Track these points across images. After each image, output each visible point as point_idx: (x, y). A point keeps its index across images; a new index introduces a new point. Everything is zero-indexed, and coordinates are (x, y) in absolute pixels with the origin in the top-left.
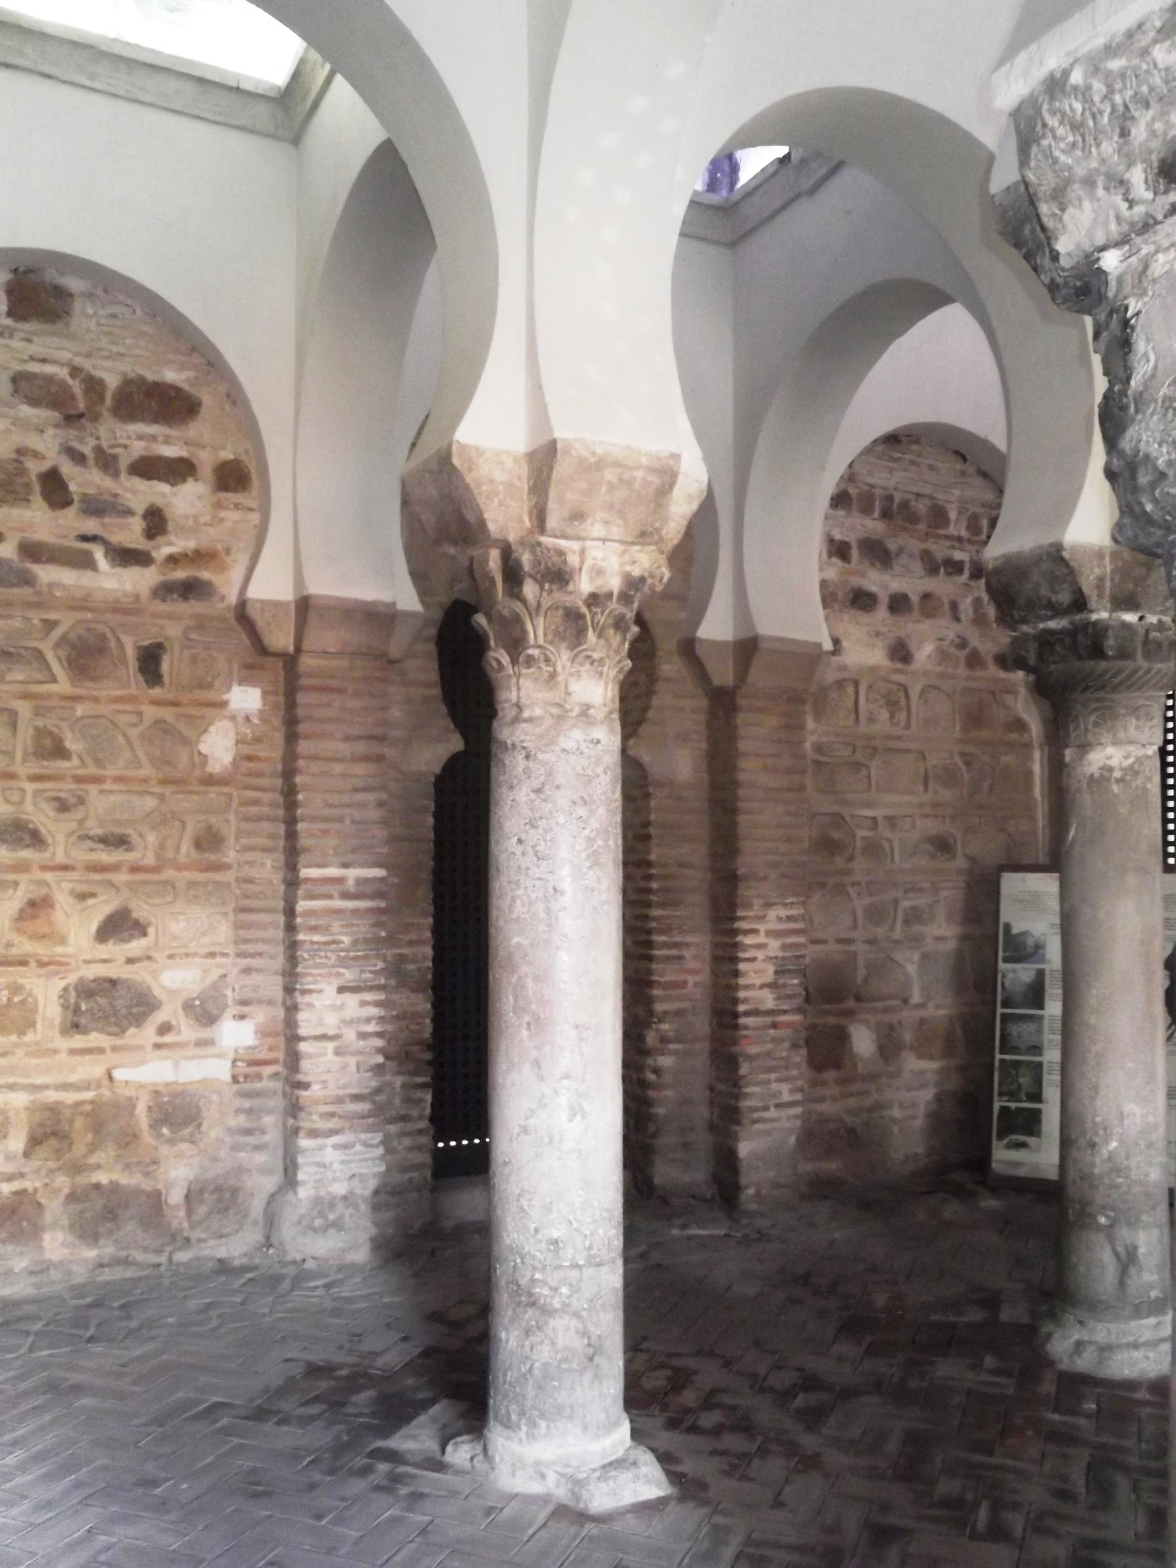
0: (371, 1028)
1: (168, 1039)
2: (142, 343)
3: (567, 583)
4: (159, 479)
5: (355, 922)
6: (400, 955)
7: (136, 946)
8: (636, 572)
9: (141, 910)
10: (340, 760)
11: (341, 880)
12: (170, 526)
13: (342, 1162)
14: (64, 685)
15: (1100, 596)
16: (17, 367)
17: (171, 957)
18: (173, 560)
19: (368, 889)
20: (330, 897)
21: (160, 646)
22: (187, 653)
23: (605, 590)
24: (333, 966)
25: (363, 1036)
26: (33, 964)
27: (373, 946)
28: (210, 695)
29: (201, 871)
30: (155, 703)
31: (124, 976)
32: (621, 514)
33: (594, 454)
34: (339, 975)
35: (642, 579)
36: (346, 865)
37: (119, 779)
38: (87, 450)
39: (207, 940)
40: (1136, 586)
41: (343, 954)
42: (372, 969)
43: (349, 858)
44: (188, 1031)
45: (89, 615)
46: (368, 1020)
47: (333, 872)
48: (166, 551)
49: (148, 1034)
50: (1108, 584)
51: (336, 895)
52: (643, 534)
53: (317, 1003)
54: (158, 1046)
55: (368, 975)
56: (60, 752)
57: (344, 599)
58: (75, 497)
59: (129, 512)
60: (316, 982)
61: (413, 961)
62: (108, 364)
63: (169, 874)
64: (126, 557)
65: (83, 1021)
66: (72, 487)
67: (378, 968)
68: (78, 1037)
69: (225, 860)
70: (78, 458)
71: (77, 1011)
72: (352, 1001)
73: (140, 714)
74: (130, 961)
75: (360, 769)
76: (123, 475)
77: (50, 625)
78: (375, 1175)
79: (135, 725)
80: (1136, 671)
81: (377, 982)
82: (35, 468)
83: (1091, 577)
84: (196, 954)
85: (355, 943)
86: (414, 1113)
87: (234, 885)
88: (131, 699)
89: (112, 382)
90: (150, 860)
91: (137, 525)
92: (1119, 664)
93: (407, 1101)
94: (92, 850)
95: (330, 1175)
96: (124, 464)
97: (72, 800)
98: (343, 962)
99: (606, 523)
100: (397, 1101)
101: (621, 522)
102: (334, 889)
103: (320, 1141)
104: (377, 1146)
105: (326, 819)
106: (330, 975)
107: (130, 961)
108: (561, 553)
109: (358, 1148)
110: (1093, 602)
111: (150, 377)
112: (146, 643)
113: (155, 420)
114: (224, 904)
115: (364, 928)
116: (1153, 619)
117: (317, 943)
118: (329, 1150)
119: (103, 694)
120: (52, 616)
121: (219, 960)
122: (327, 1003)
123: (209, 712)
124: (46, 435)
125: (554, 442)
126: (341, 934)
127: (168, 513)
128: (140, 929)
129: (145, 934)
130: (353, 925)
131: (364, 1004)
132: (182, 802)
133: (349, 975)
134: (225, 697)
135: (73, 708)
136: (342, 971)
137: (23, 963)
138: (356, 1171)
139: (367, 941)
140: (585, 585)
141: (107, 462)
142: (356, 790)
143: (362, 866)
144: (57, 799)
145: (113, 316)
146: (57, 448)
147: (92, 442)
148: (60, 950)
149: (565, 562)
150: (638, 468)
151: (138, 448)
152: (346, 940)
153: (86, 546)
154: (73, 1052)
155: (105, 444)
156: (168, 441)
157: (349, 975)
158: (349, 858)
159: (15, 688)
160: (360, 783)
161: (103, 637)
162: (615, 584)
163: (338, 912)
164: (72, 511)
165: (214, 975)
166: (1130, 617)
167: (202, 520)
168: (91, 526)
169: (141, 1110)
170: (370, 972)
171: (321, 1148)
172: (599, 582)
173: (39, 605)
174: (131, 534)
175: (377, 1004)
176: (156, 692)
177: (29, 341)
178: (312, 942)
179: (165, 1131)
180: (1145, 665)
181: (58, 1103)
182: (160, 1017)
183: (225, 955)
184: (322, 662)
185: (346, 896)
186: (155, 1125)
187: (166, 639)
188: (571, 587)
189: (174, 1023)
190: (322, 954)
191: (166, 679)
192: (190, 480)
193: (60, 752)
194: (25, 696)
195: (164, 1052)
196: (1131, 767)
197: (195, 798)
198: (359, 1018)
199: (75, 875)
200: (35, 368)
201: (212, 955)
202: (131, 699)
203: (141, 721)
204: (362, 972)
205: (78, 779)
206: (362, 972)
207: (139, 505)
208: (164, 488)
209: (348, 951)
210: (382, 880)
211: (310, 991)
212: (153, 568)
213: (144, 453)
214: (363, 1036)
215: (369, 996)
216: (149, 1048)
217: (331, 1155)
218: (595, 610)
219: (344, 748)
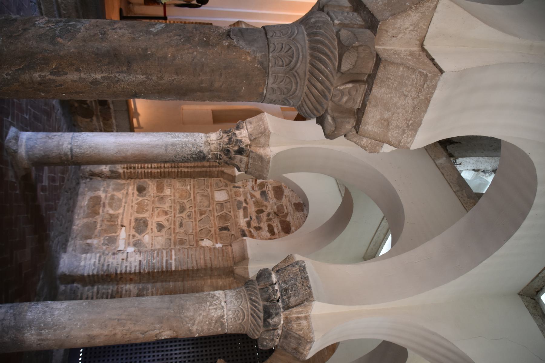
0: (128, 269)
1: (131, 237)
2: (298, 223)
3: (237, 129)
4: (268, 229)
5: (159, 263)
6: (149, 289)
7: (155, 230)
8: (243, 140)
9: (164, 231)
10: (204, 257)
11: (171, 259)
12: (258, 232)
13: (90, 264)
14: (216, 214)
16: (284, 204)
17: (152, 236)
18: (250, 232)
19: (169, 266)
20: (167, 257)
21: (229, 230)
22: (228, 235)
23: (237, 136)
24: (147, 258)
25: (126, 267)
26: (152, 212)
27: (152, 268)
28: (218, 240)
29: (174, 241)
30: (215, 230)
31: (148, 228)
32: (254, 129)
33: (264, 118)
34: (145, 260)
35: (242, 142)
36: (175, 259)
37: (196, 225)
38: (271, 217)
39: (156, 243)
41: (150, 261)
42: (146, 268)
43: (177, 260)
44: (132, 240)
45: (233, 218)
46: (131, 268)
47: (174, 257)
48: (252, 230)
49: (133, 232)
51: (167, 258)
52: (251, 135)
53: (137, 256)
54: (129, 235)
55: (144, 267)
56: (201, 214)
57: (247, 247)
58: (259, 215)
59: (259, 224)
60: (143, 255)
61: (146, 293)
62: (291, 218)
63: (173, 235)
64: (249, 224)
65: (138, 221)
66: (261, 214)
67: (146, 269)
68: (134, 220)
69: (177, 246)
70: (268, 215)
71: (140, 220)
72: (137, 264)
73: (212, 227)
74: (152, 229)
75: (202, 262)
76: (267, 222)
77: (230, 212)
78: (84, 272)
79: (209, 226)
81: (141, 269)
82: (264, 208)
84: (152, 241)
85: (154, 263)
86: (99, 295)
87: (170, 248)
88: (215, 226)
89: (288, 219)
90: (176, 231)
91: (257, 225)
93: (103, 293)
94: (179, 221)
95: (87, 261)
96: (270, 223)
97: (190, 217)
98: (148, 261)
99: (251, 128)
100: (104, 291)
101: (252, 130)
102: (169, 257)
103: (98, 258)
104: (93, 272)
105: (188, 254)
106: (145, 258)
107: (152, 229)
108: (243, 127)
109: (93, 267)
111: (291, 225)
112: (229, 227)
113: (281, 227)
114: (165, 246)
115: (158, 265)
116: (276, 287)
117: (154, 255)
118: (94, 260)
119: (216, 221)
120: (232, 212)
121: (150, 246)
122: (137, 258)
123: (214, 240)
124: (270, 210)
125: (264, 112)
126: (156, 260)
127: (261, 231)
128: (159, 231)
129: (158, 231)
130: (158, 262)
131: (136, 267)
132: (191, 237)
133: (144, 262)
134: (219, 243)
135: (212, 216)
136: (146, 261)
137: (153, 211)
138: (86, 267)
139: (154, 266)
140: (237, 132)
141: (269, 220)
142: (196, 261)
143: (175, 263)
144: (191, 215)
145: (302, 218)
146: (269, 211)
147: (273, 218)
148: (155, 217)
149: (241, 128)
150: (264, 125)
151: (274, 225)
152: (154, 261)
153: (249, 217)
154: (131, 220)
155: (273, 220)
156: (278, 229)
157: (144, 262)
158: (177, 260)
159: (215, 207)
160: (198, 262)
161: (229, 221)
162: (239, 137)
163: (162, 259)
164: (255, 214)
165: (147, 245)
167: (261, 236)
168: (254, 217)
169: (113, 234)
170: (145, 268)
171: (95, 258)
172: (239, 134)
173: (234, 210)
174: (254, 223)
175: (135, 270)
176: (218, 230)
177: (290, 205)
178: (154, 253)
179: (107, 238)
180: (258, 290)
181: (119, 218)
182: (137, 235)
183: (152, 247)
184: (230, 252)
185: (167, 261)
186: (110, 237)
187: (231, 232)
188: (236, 130)
189: (135, 238)
190: (151, 256)
191: (221, 232)
192: (270, 234)
193: (201, 214)
194: (213, 209)
195: (128, 236)
196: (215, 296)
197: (193, 239)
198: (131, 265)
199: (173, 219)
200: (285, 207)
201: (152, 244)
202: (215, 226)
203: (211, 228)
204: (145, 266)
205: (195, 218)
206: (145, 266)
207: (262, 225)
208: (267, 229)
209: (151, 262)
210: (171, 268)
211: (140, 254)
212: (247, 228)
213: (274, 226)
214: (126, 267)
215: (137, 268)
216: (129, 233)
217: (93, 261)
218: (232, 134)
219: (208, 258)
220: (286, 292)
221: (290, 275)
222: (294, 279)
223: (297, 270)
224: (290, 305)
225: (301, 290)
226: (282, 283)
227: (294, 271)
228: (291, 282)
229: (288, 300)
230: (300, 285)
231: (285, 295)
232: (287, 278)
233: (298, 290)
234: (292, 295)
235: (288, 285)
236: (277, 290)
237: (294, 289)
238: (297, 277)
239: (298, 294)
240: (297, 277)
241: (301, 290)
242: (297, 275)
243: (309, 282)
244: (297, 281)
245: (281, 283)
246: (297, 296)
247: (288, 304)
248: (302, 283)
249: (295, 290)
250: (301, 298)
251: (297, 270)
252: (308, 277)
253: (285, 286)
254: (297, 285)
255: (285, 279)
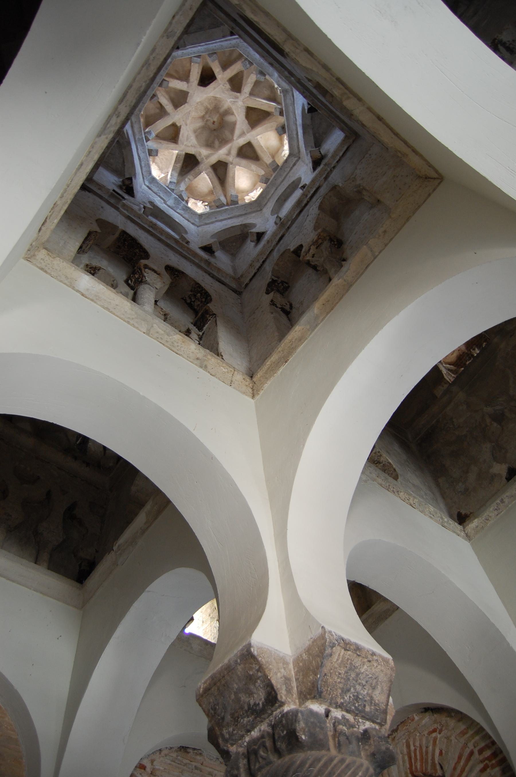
15: (289, 691)
40: (316, 675)
50: (294, 684)
80: (331, 760)
83: (279, 674)
92: (314, 754)
110: (282, 695)
166: (318, 708)
220: (360, 699)
221: (340, 674)
222: (350, 669)
223: (342, 654)
224: (383, 706)
225: (373, 671)
226: (344, 698)
227: (338, 660)
228: (351, 678)
229: (375, 705)
230: (365, 667)
231: (365, 706)
232: (340, 682)
233: (371, 676)
234: (370, 692)
235: (352, 689)
236: (343, 717)
237: (364, 683)
238: (351, 663)
239: (375, 681)
240: (351, 663)
241: (373, 671)
242: (348, 659)
243: (364, 648)
244: (356, 668)
245: (342, 700)
246: (377, 684)
247: (380, 709)
248: (366, 660)
249: (367, 682)
250: (385, 679)
251: (342, 654)
252: (356, 644)
253: (351, 695)
254: (362, 670)
255: (340, 688)
